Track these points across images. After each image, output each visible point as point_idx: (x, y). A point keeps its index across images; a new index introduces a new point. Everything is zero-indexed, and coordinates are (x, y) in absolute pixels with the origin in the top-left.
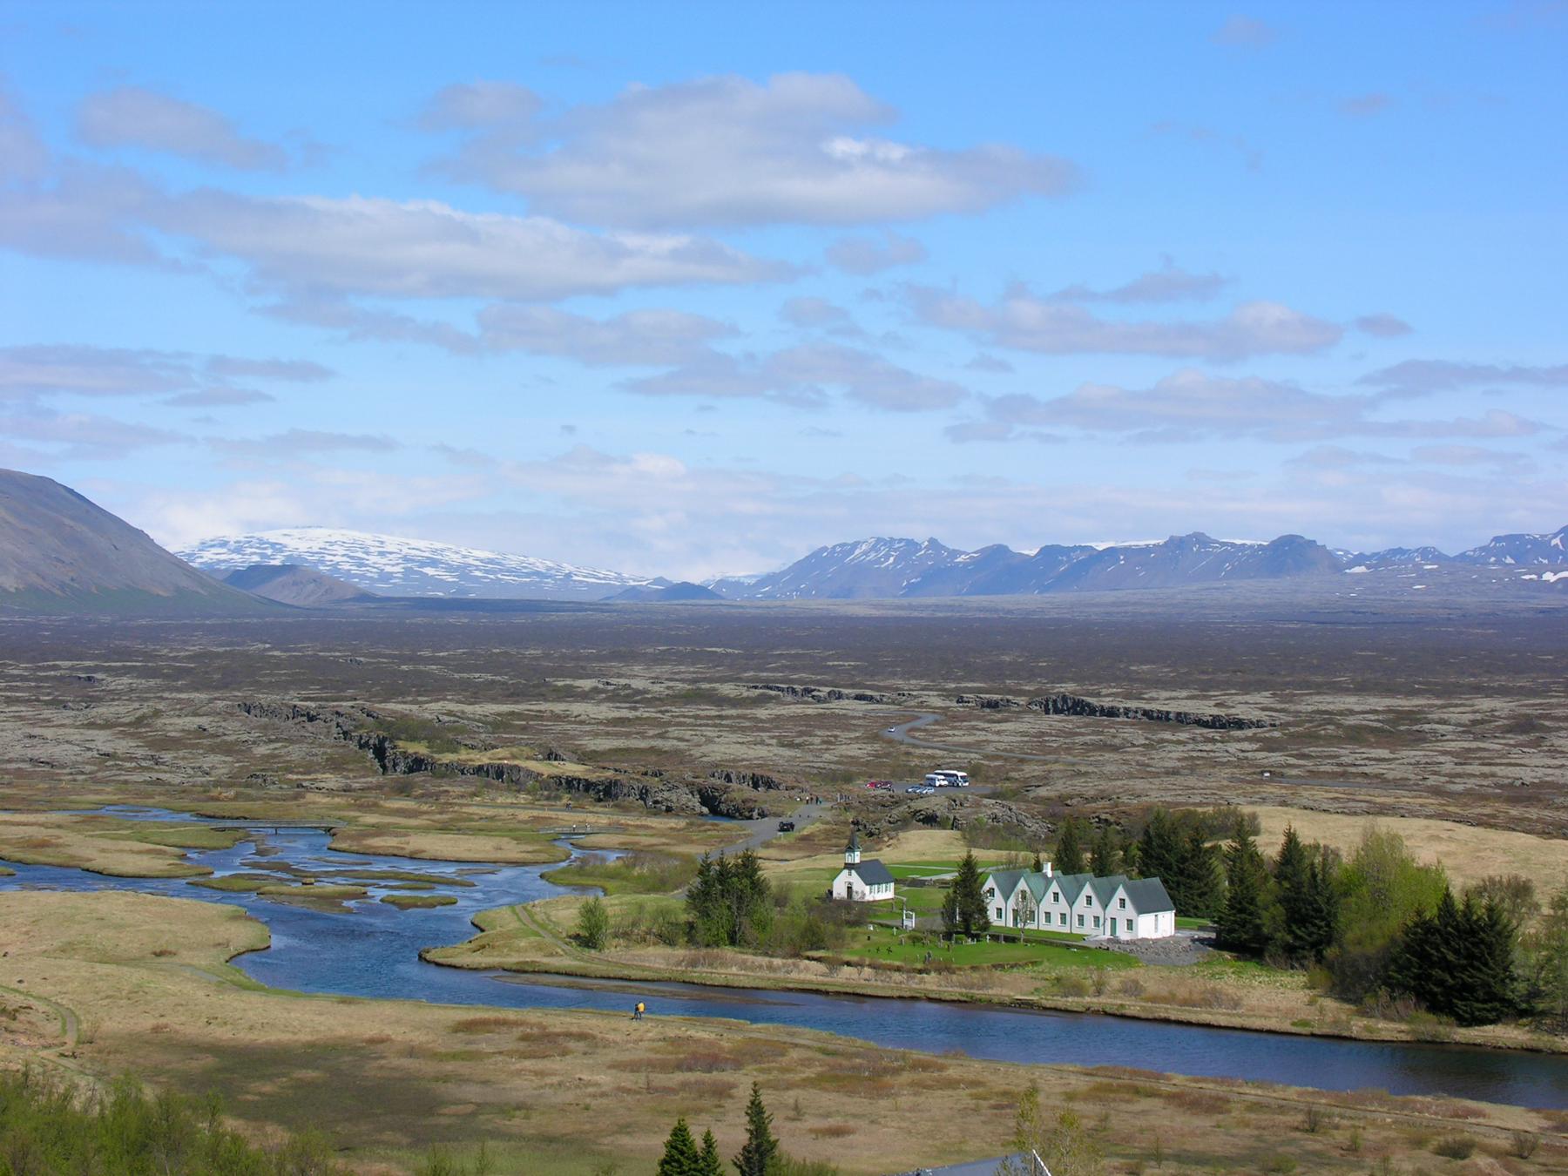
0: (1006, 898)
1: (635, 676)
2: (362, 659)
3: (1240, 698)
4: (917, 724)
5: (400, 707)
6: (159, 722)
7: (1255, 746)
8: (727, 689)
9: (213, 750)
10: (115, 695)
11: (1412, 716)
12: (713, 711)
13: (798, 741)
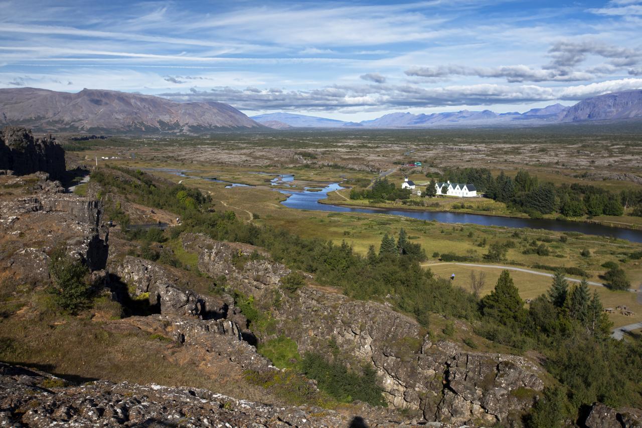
0: (440, 188)
6: (254, 154)
8: (369, 145)
9: (266, 159)
10: (244, 148)
11: (518, 149)
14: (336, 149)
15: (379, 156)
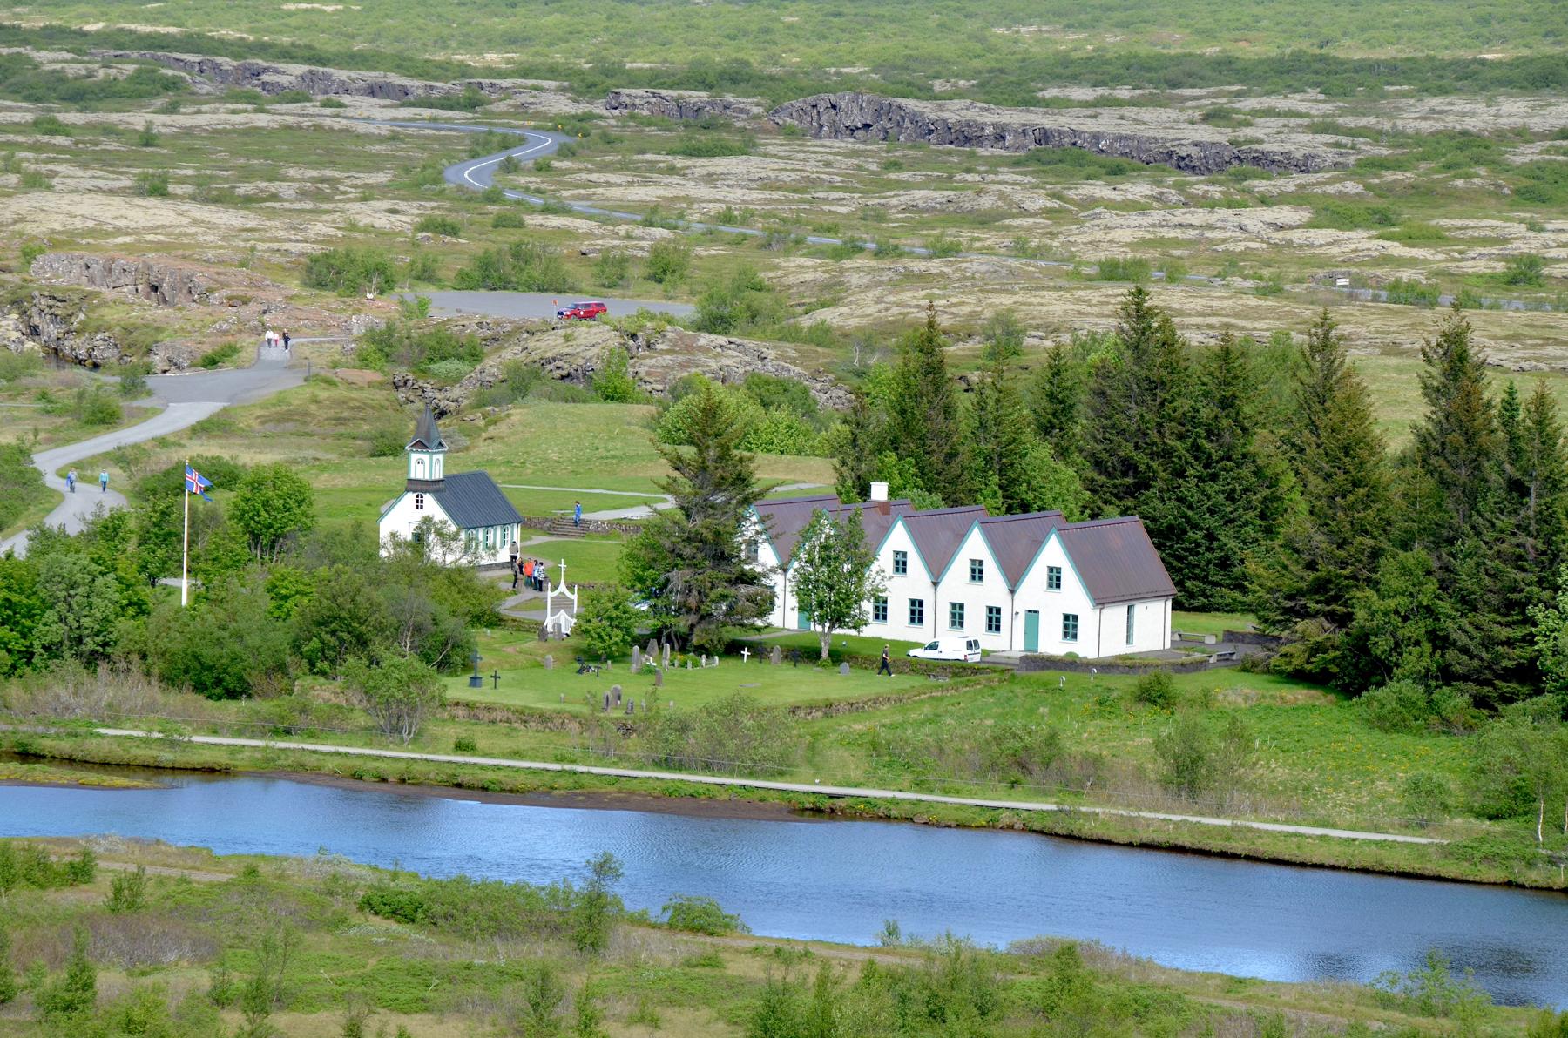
4: (516, 154)
13: (244, 189)
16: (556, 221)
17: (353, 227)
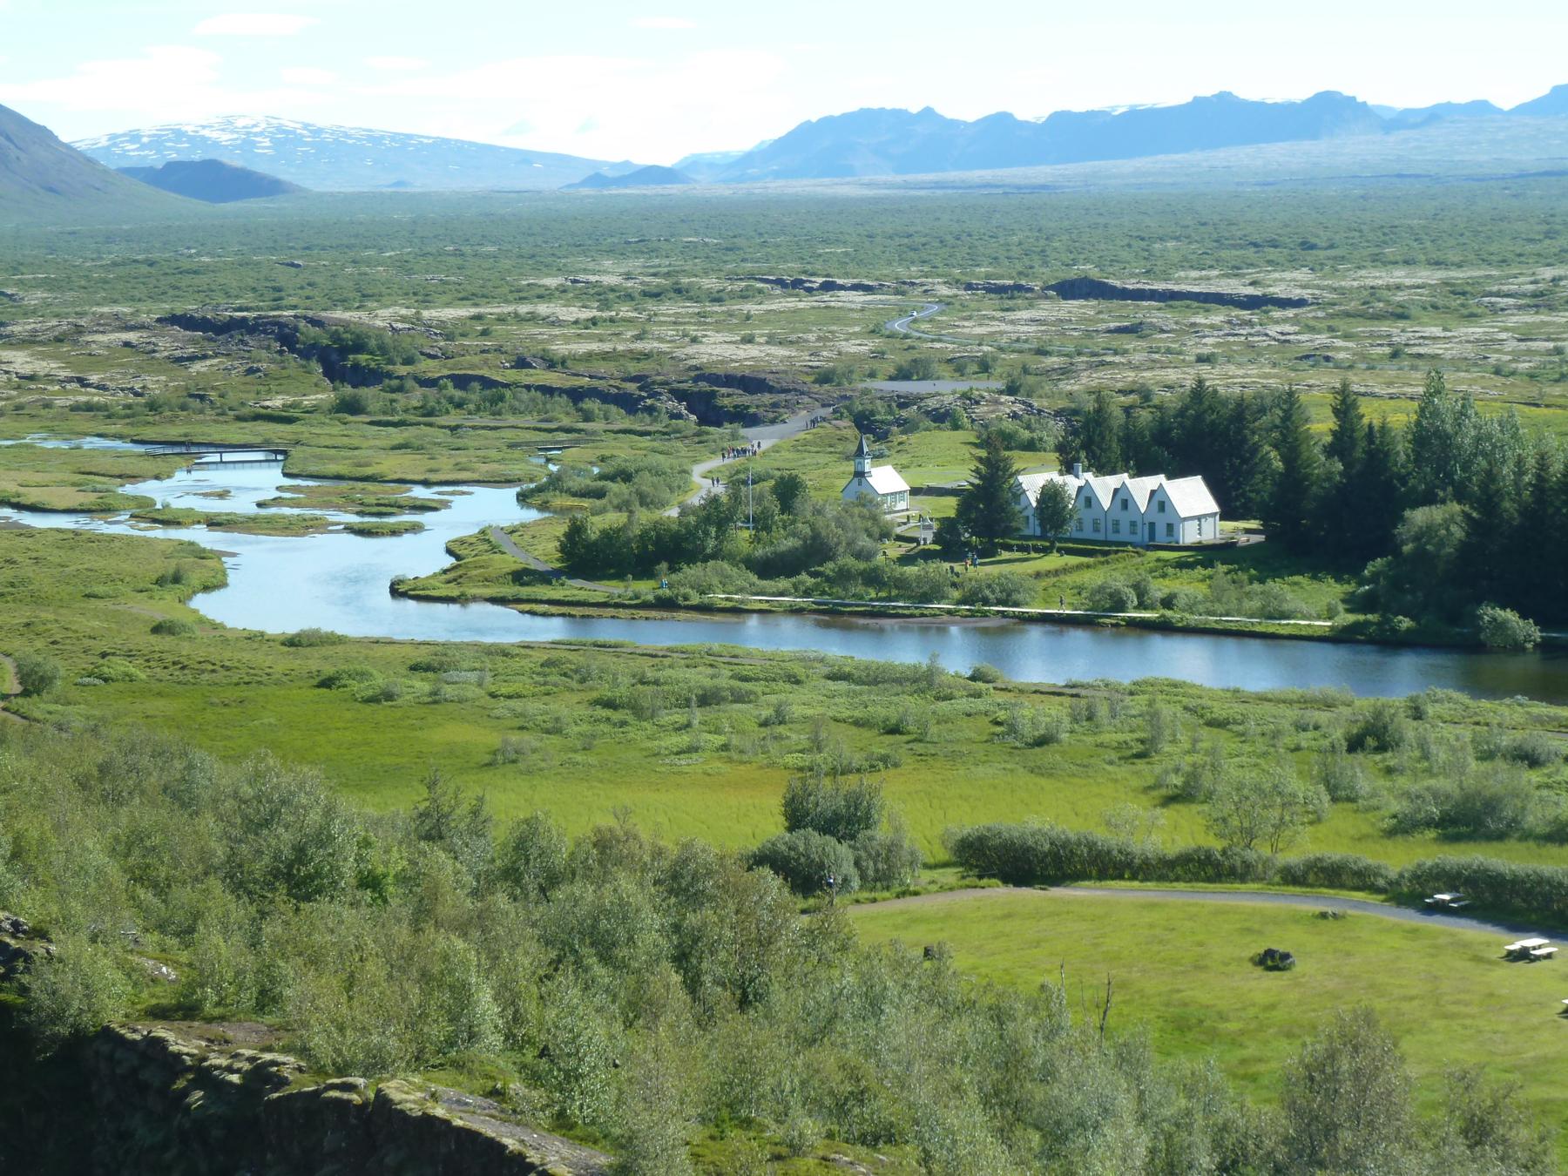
1: (606, 272)
2: (300, 263)
3: (1277, 275)
5: (347, 315)
7: (1296, 328)
8: (710, 283)
12: (694, 308)
13: (793, 337)
14: (524, 309)
15: (749, 340)
16: (938, 345)
17: (840, 354)
